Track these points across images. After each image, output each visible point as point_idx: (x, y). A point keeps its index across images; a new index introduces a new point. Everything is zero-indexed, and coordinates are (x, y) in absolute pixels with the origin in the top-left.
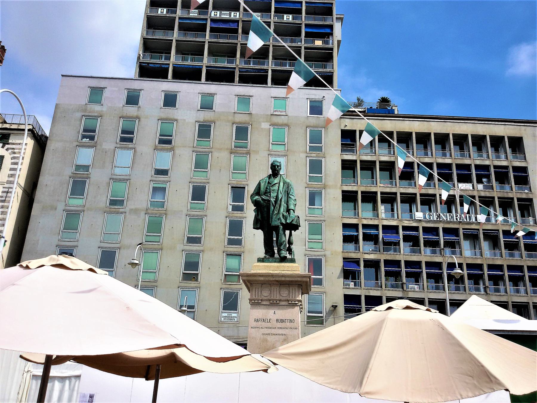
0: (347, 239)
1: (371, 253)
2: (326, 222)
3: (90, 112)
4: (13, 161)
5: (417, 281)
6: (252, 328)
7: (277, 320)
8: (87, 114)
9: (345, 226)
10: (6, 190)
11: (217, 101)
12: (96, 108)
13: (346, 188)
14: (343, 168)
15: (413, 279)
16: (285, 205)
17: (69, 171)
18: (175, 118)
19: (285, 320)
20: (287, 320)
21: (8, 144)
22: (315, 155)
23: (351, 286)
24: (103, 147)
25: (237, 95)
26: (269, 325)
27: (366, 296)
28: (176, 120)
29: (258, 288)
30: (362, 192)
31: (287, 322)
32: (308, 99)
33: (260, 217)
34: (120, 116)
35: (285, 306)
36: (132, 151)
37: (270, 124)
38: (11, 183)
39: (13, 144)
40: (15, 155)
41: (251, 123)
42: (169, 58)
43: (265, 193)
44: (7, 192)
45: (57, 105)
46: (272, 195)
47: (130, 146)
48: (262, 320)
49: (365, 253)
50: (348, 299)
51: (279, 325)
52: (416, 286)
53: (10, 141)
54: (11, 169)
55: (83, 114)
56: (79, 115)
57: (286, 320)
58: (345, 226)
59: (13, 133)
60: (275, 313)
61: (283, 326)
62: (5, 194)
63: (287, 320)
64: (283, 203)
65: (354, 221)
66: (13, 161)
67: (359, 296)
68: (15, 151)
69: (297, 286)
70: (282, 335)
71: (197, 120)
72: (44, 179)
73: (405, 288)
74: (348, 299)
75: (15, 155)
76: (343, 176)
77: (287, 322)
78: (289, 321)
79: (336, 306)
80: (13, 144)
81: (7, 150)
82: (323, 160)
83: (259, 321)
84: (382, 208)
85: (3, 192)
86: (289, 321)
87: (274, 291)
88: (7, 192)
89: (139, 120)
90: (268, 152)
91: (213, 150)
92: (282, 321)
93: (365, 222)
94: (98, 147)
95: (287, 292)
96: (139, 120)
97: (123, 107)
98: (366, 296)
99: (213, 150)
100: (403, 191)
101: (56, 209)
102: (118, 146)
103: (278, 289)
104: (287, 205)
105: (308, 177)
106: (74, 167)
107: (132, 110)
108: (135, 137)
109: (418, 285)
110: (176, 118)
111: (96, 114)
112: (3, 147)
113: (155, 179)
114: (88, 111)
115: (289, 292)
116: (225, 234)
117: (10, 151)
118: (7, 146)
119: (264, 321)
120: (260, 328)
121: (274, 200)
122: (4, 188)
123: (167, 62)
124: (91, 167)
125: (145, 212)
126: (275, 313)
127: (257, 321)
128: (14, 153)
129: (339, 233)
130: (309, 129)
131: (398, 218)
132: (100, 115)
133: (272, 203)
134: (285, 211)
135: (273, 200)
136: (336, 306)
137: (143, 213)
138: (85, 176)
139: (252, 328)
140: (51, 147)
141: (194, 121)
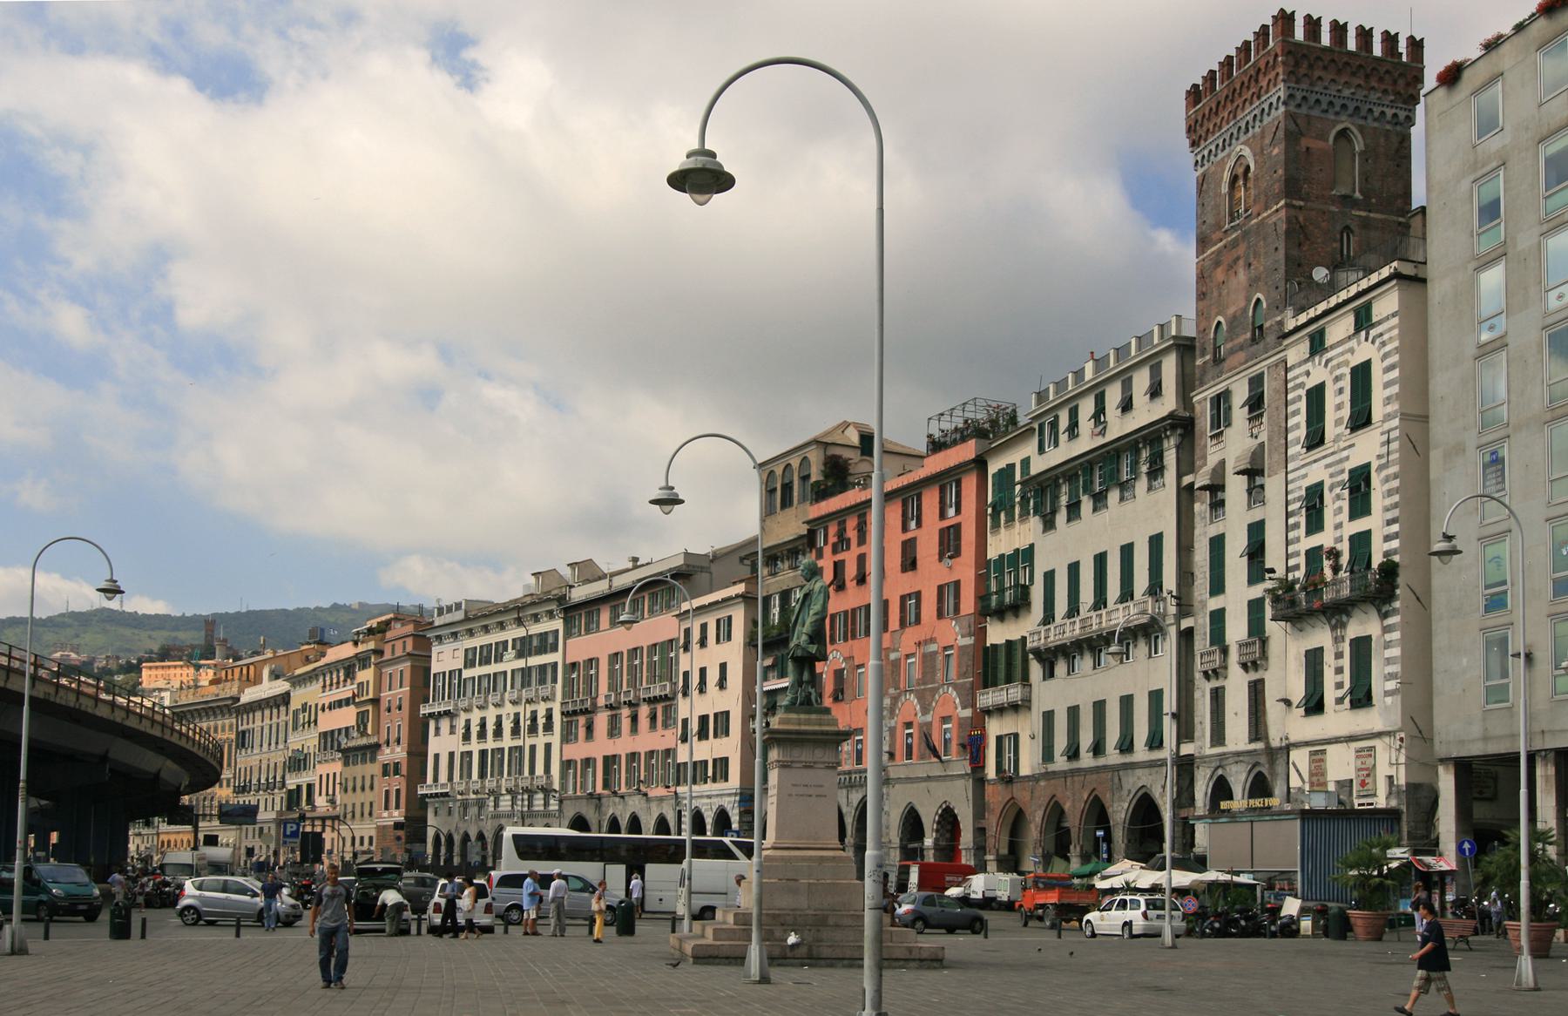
3: (1483, 166)
8: (1480, 173)
10: (1385, 438)
24: (1520, 248)
34: (1537, 139)
44: (1388, 442)
53: (1374, 319)
55: (1472, 178)
59: (1373, 298)
81: (1373, 342)
85: (1383, 444)
88: (1388, 442)
94: (1509, 255)
101: (1464, 450)
111: (1494, 164)
112: (1367, 339)
114: (1479, 165)
118: (1373, 333)
128: (1383, 344)
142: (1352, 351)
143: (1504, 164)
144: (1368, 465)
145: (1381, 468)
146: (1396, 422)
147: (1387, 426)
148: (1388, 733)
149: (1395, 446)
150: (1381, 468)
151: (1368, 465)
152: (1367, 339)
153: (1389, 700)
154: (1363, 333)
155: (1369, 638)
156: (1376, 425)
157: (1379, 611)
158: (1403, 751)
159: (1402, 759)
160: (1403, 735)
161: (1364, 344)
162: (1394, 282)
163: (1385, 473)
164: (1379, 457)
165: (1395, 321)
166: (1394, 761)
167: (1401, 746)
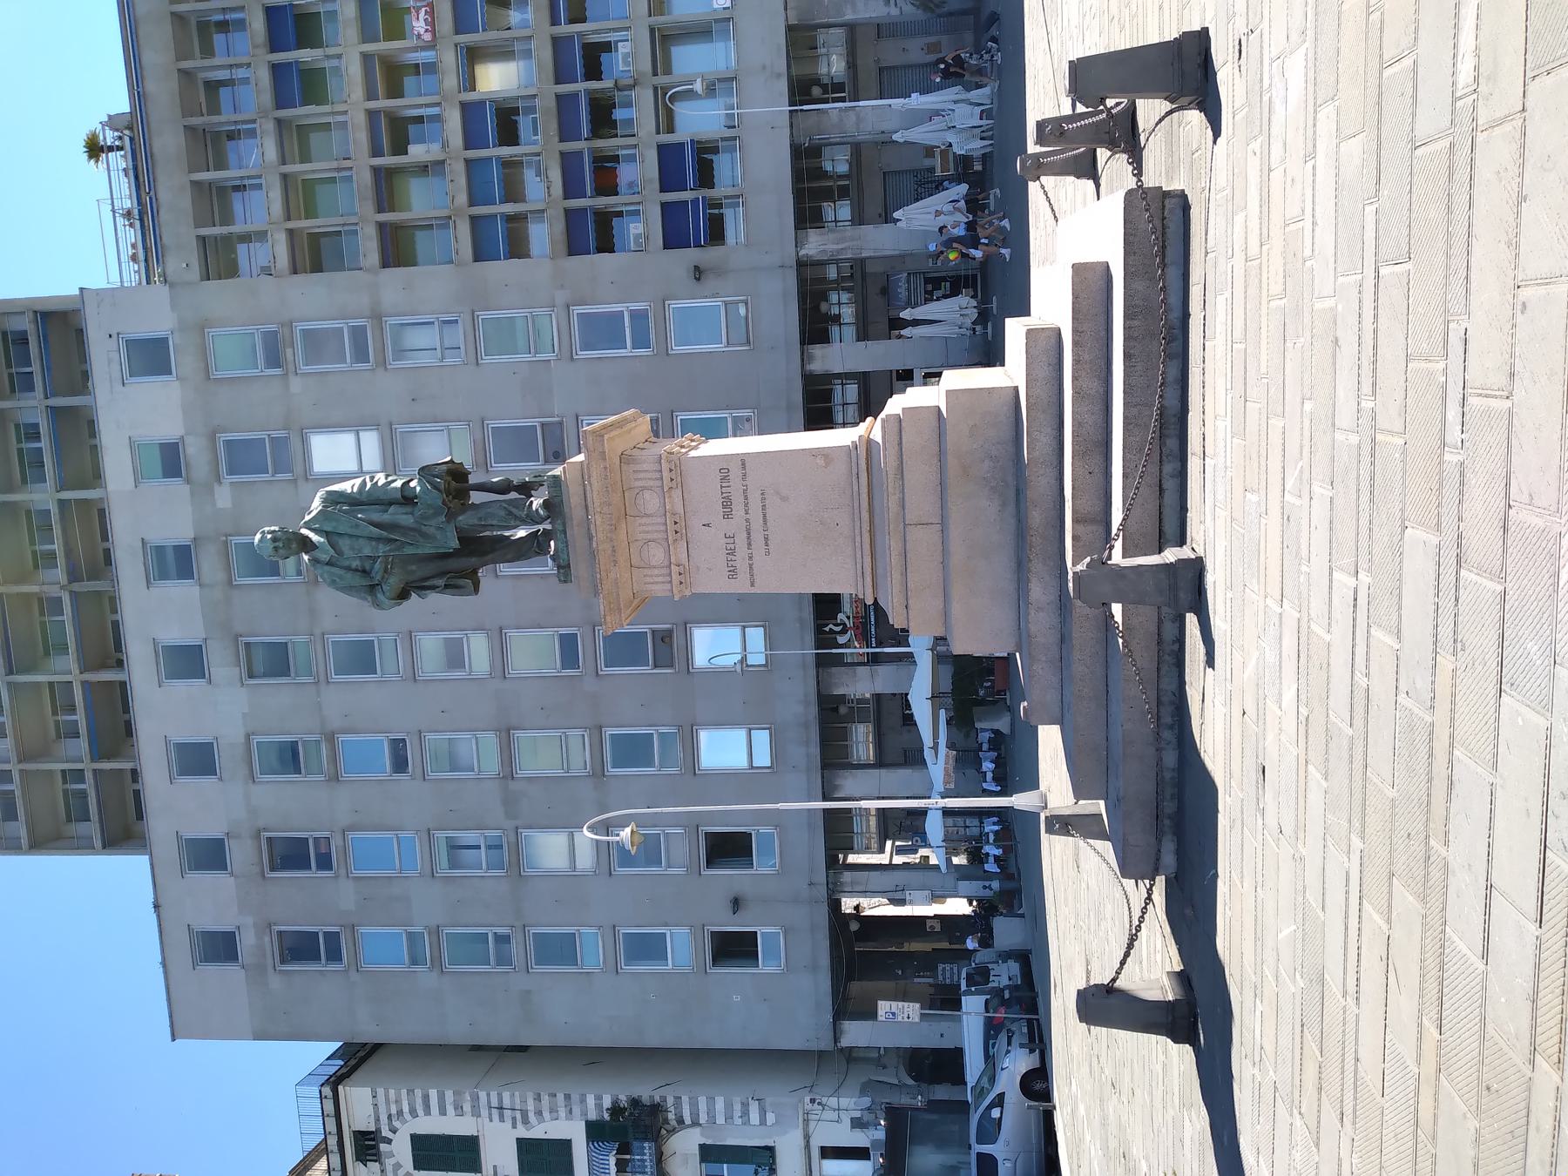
0: (517, 248)
1: (547, 178)
2: (476, 308)
4: (420, 1112)
5: (607, 47)
6: (752, 585)
7: (727, 516)
8: (269, 961)
9: (481, 254)
10: (495, 1113)
11: (176, 635)
12: (247, 942)
13: (373, 258)
14: (317, 267)
15: (604, 57)
16: (392, 509)
17: (426, 977)
18: (243, 741)
19: (724, 495)
20: (724, 490)
21: (378, 1130)
22: (289, 351)
23: (641, 230)
25: (148, 582)
26: (741, 539)
27: (662, 190)
28: (248, 736)
29: (645, 576)
30: (380, 210)
31: (728, 490)
32: (125, 381)
33: (441, 582)
35: (685, 497)
36: (351, 835)
37: (216, 486)
38: (477, 1106)
39: (377, 1120)
40: (406, 1109)
41: (224, 538)
42: (79, 775)
43: (365, 572)
44: (501, 1108)
45: (258, 1036)
46: (367, 551)
47: (340, 843)
48: (730, 557)
49: (549, 196)
50: (674, 238)
51: (738, 510)
52: (621, 50)
54: (443, 1112)
56: (275, 982)
57: (722, 493)
58: (481, 254)
59: (350, 1127)
60: (708, 525)
61: (742, 499)
62: (507, 1113)
63: (724, 490)
64: (386, 517)
65: (464, 230)
66: (420, 1112)
67: (665, 206)
68: (394, 1111)
69: (624, 467)
70: (763, 499)
71: (239, 684)
72: (459, 1031)
73: (631, 82)
74: (674, 238)
75: (406, 1109)
76: (340, 267)
77: (728, 490)
78: (724, 485)
79: (697, 268)
80: (377, 1120)
82: (299, 327)
83: (732, 566)
84: (417, 152)
85: (502, 1119)
86: (724, 485)
87: (648, 532)
88: (501, 1108)
89: (265, 830)
90: (301, 482)
91: (318, 631)
92: (727, 504)
93: (462, 198)
95: (647, 494)
96: (265, 830)
97: (236, 877)
98: (662, 190)
99: (318, 631)
100: (358, 92)
101: (529, 992)
102: (343, 872)
103: (639, 520)
104: (391, 504)
105: (280, 476)
106: (418, 968)
107: (241, 854)
108: (312, 833)
109: (616, 42)
110: (242, 739)
111: (267, 939)
112: (389, 1141)
113: (419, 771)
115: (644, 488)
116: (542, 576)
117: (396, 1124)
118: (385, 1133)
119: (732, 554)
120: (751, 562)
121: (381, 546)
122: (491, 1121)
123: (89, 776)
124: (410, 929)
125: (510, 782)
126: (708, 525)
127: (733, 573)
128: (400, 1113)
129: (501, 270)
130: (215, 373)
131: (438, 104)
132: (268, 930)
133: (390, 551)
134: (408, 509)
135: (382, 549)
136: (697, 268)
137: (513, 785)
138: (434, 938)
139: (752, 585)
140: (369, 1032)
141: (243, 689)
142: (398, 1166)
143: (270, 925)
144: (520, 1141)
145: (526, 1121)
146: (483, 1095)
147: (484, 1112)
148: (806, 1122)
149: (507, 1102)
150: (526, 1121)
151: (520, 1141)
152: (389, 1141)
153: (771, 1118)
154: (383, 1147)
155: (703, 1147)
156: (481, 1129)
157: (673, 1131)
158: (824, 1100)
159: (833, 1101)
160: (807, 1099)
161: (394, 1147)
162: (340, 1088)
163: (531, 1116)
164: (514, 1126)
165: (381, 1092)
166: (834, 1116)
167: (819, 1104)
